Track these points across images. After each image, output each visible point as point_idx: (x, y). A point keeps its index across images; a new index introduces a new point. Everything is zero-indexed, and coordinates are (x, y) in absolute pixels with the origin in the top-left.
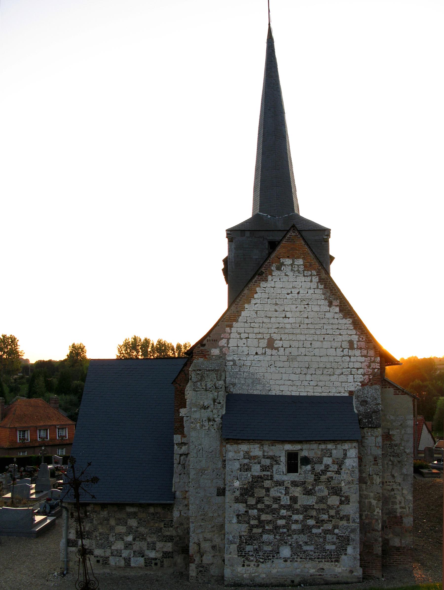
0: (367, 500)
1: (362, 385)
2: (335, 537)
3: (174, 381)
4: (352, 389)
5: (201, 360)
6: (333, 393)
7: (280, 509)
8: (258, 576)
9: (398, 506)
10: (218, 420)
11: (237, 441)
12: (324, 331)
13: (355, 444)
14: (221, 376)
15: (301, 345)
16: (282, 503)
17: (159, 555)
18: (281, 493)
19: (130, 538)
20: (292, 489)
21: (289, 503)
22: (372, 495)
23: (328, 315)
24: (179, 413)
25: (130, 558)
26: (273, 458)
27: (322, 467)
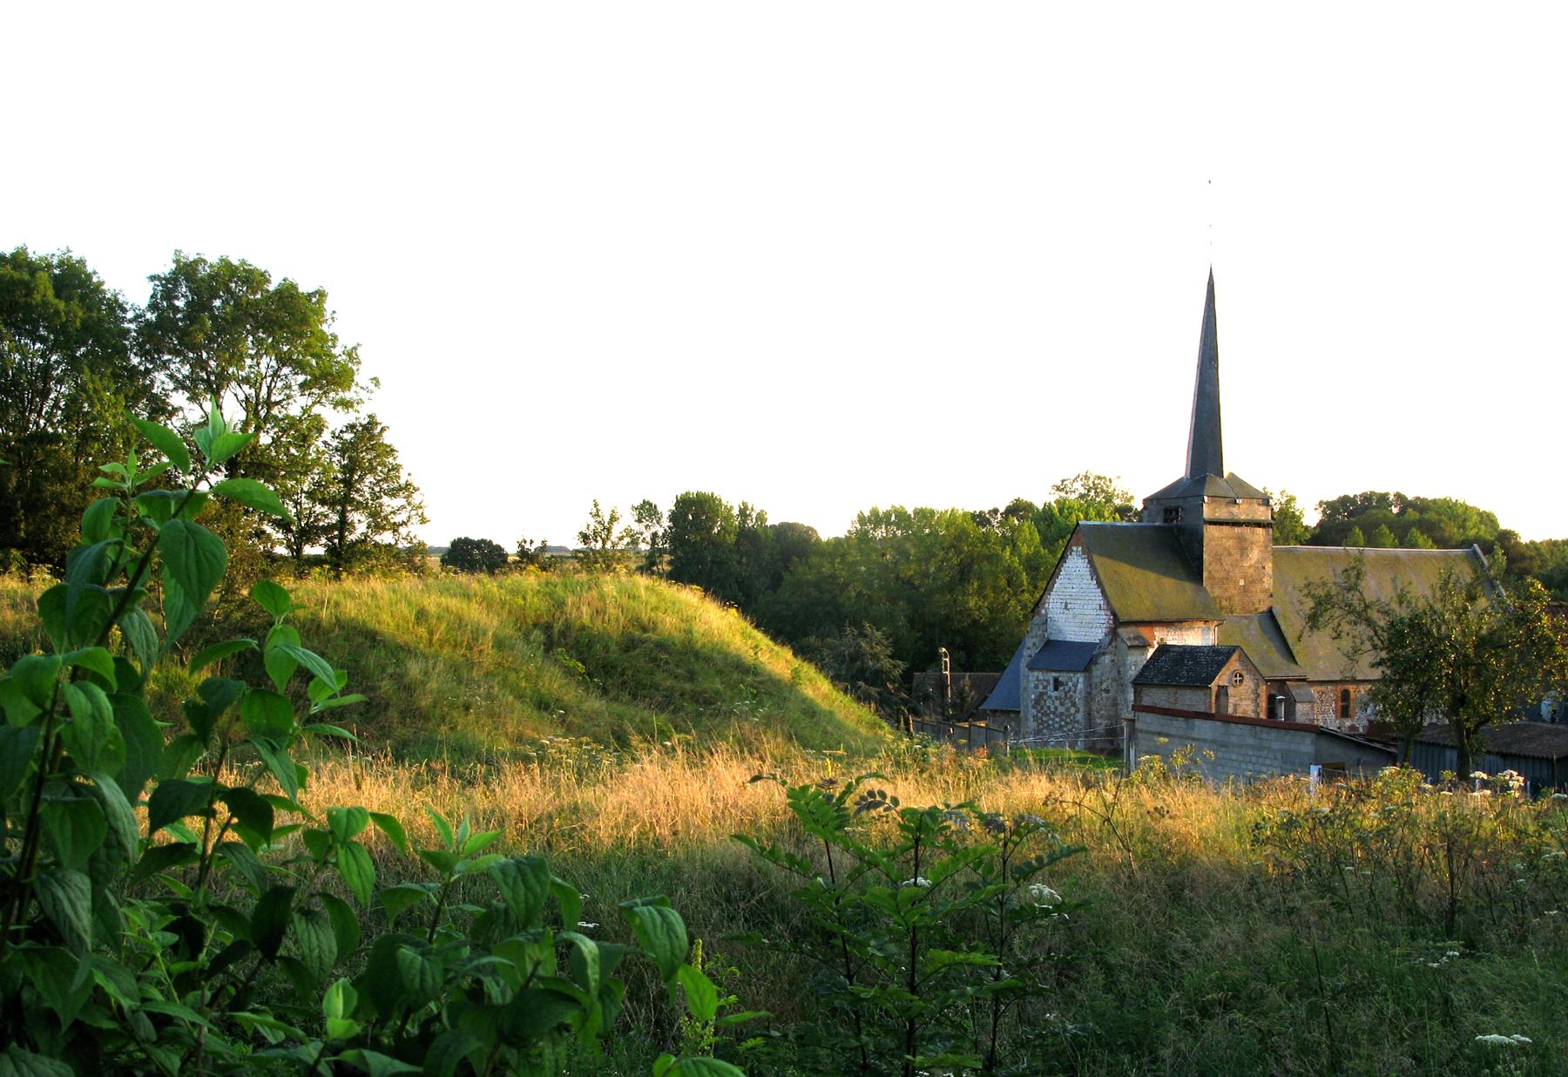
26: (1048, 681)
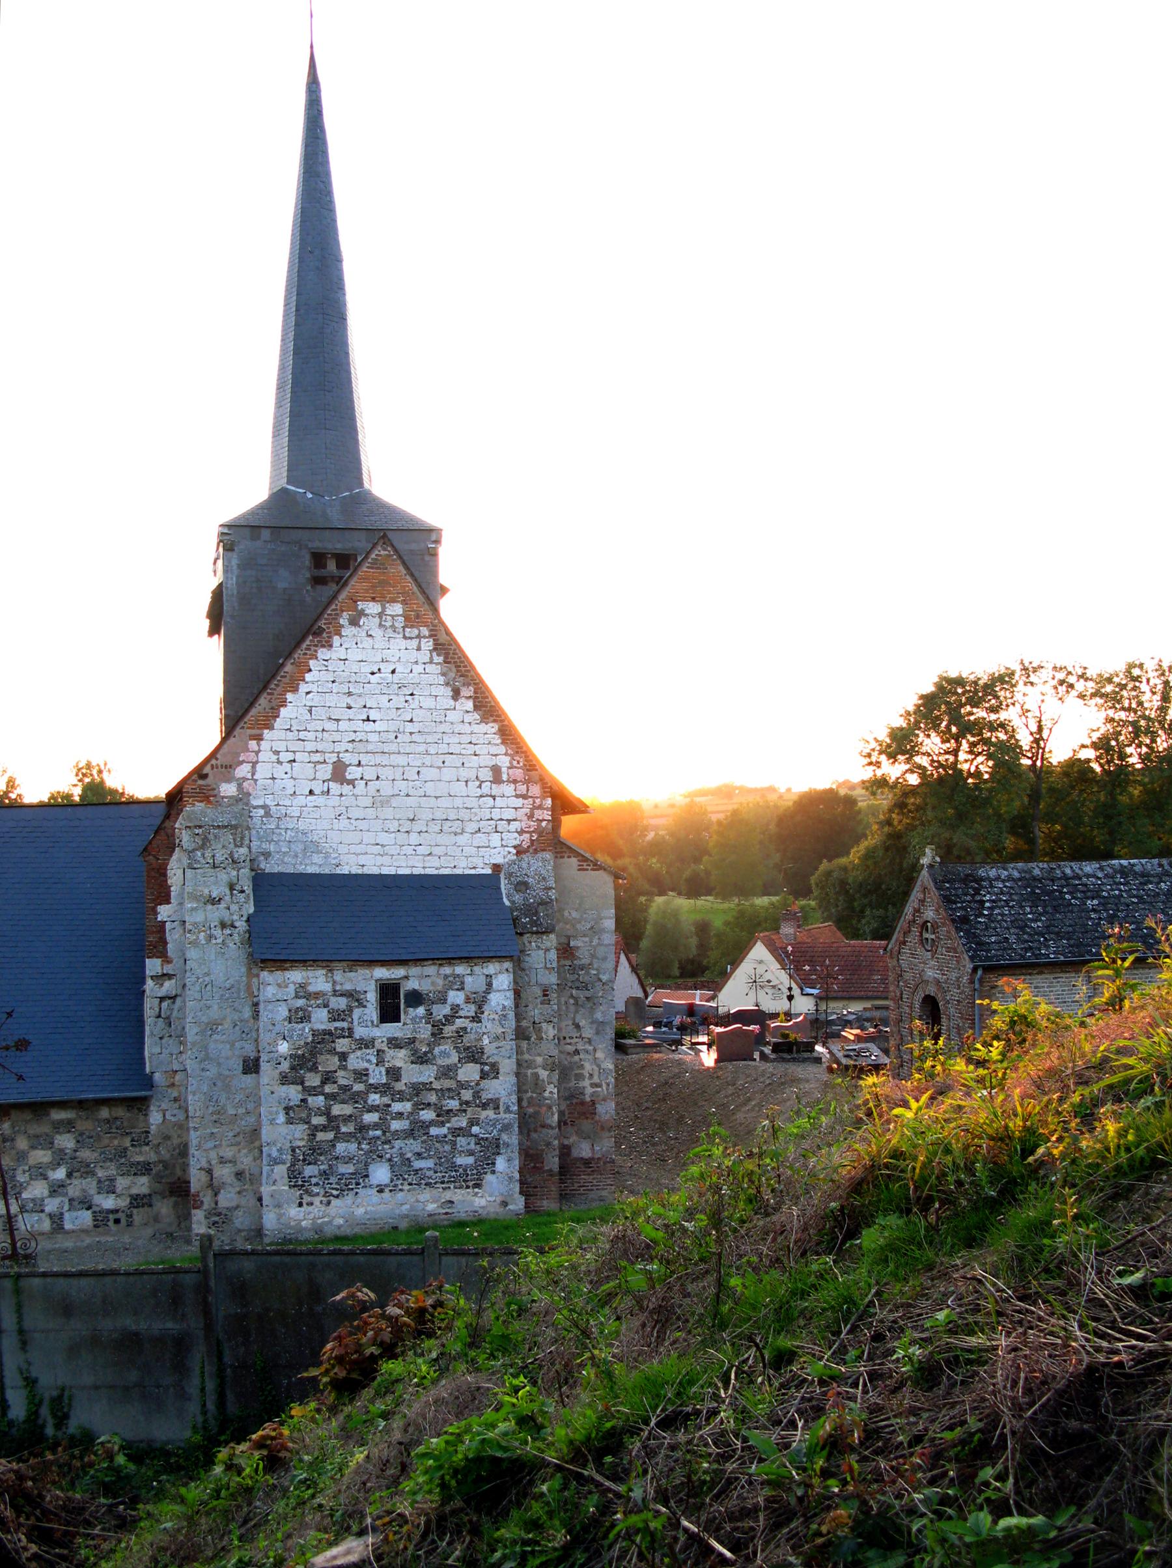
0: (530, 1071)
1: (518, 853)
2: (473, 1140)
3: (145, 849)
4: (499, 860)
5: (200, 806)
6: (462, 867)
7: (367, 1093)
8: (330, 1222)
9: (586, 1083)
10: (241, 925)
11: (280, 963)
12: (443, 748)
13: (508, 965)
14: (242, 838)
15: (398, 776)
16: (371, 1081)
17: (123, 1203)
18: (369, 1061)
19: (60, 1174)
20: (390, 1053)
21: (384, 1081)
22: (539, 1060)
23: (452, 716)
24: (156, 913)
25: (62, 1214)
27: (446, 1010)
